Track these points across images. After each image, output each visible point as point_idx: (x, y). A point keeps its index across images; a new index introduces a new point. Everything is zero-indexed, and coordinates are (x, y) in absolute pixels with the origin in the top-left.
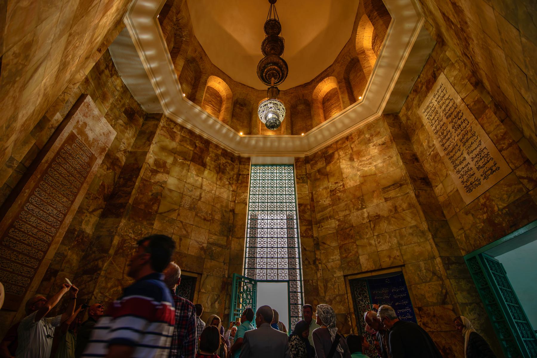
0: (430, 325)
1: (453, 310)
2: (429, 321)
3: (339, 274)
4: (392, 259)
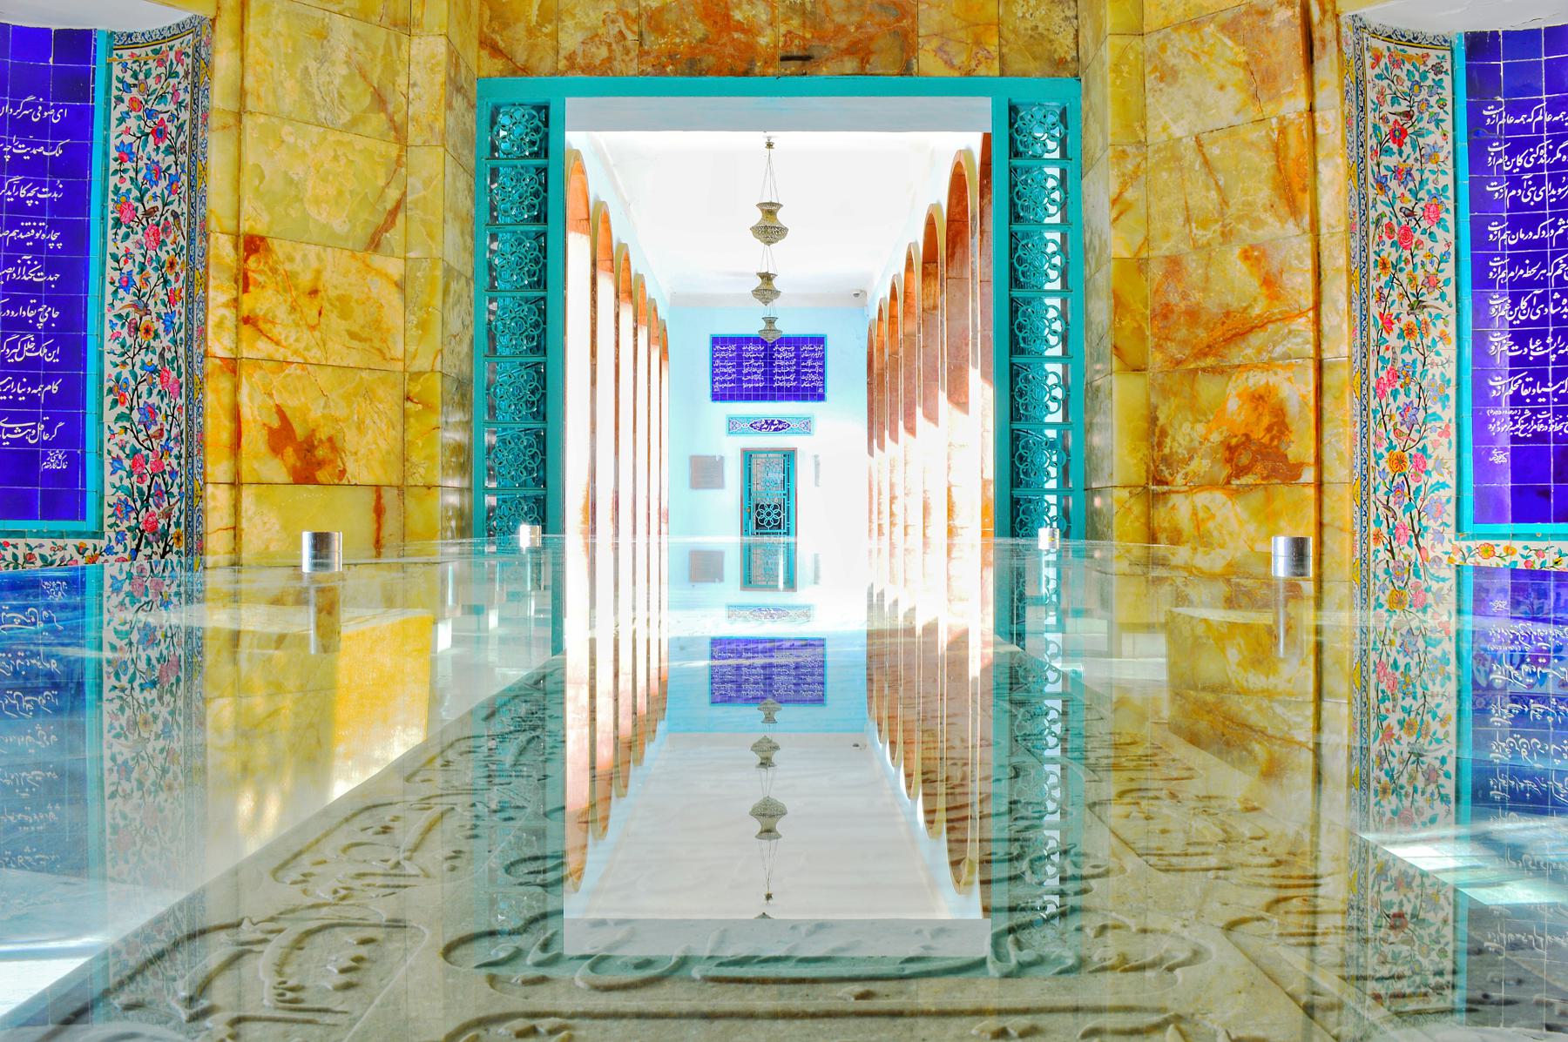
0: (276, 332)
1: (401, 286)
2: (282, 313)
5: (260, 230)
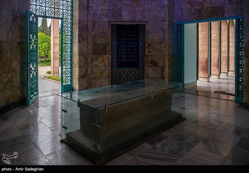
1: (164, 47)
3: (106, 19)
4: (142, 17)
5: (150, 43)
